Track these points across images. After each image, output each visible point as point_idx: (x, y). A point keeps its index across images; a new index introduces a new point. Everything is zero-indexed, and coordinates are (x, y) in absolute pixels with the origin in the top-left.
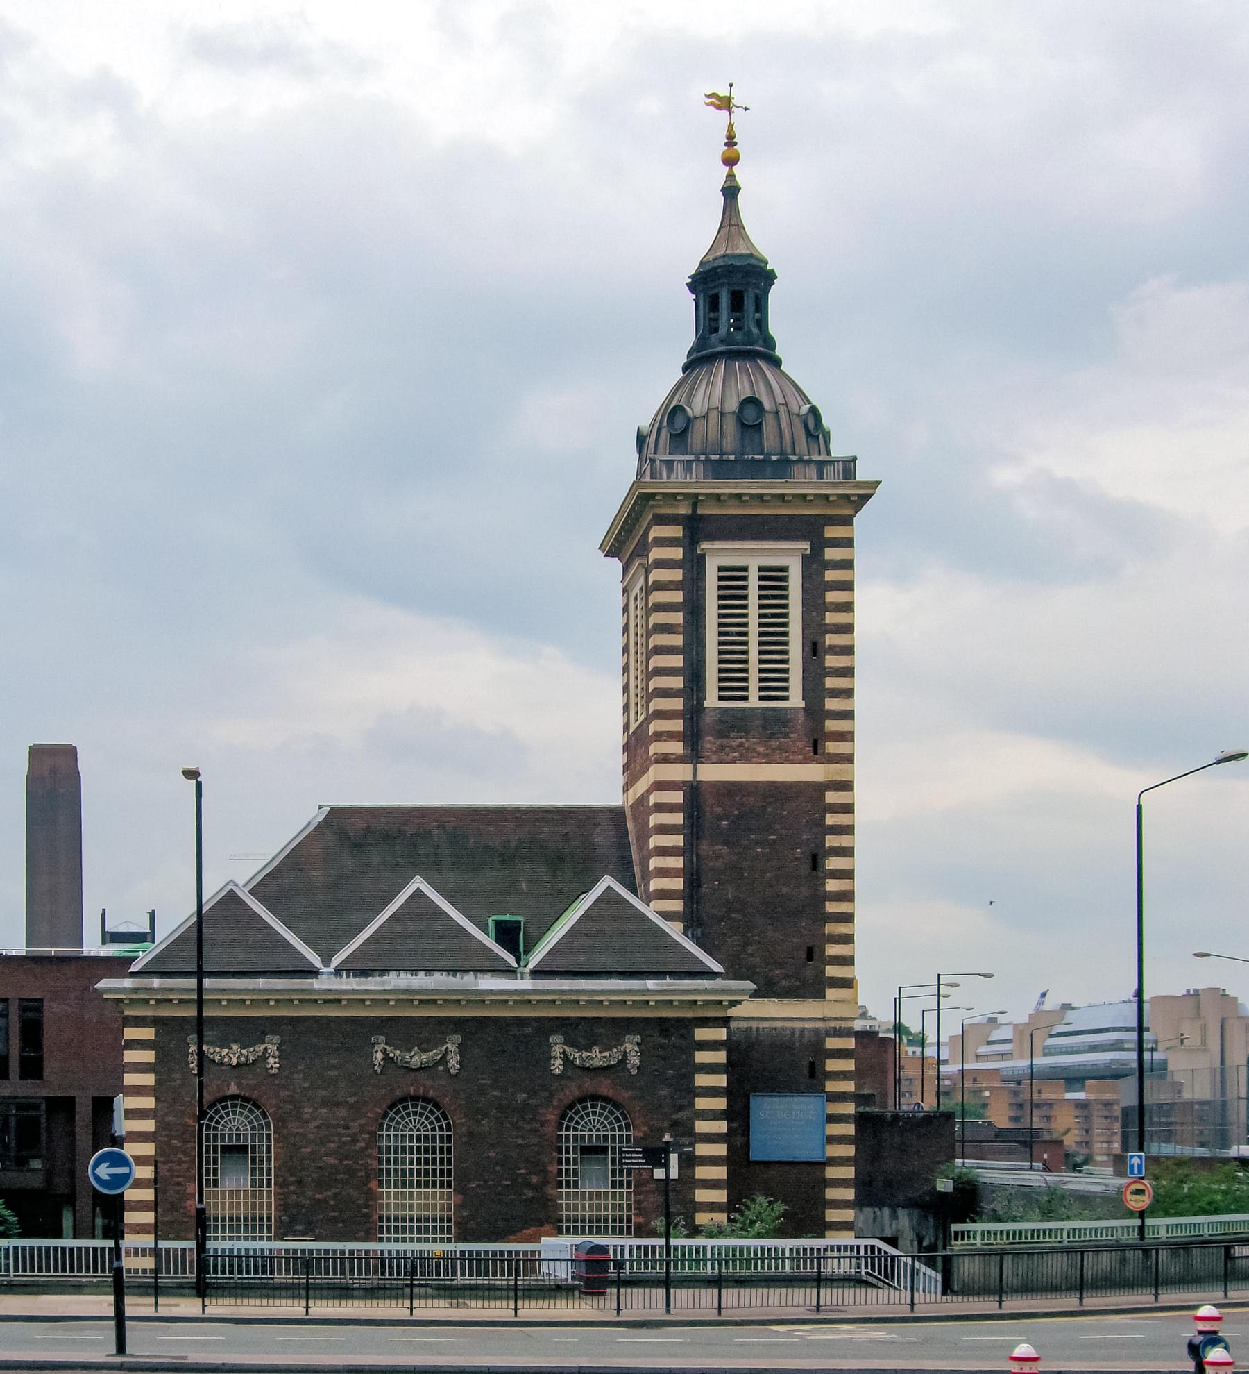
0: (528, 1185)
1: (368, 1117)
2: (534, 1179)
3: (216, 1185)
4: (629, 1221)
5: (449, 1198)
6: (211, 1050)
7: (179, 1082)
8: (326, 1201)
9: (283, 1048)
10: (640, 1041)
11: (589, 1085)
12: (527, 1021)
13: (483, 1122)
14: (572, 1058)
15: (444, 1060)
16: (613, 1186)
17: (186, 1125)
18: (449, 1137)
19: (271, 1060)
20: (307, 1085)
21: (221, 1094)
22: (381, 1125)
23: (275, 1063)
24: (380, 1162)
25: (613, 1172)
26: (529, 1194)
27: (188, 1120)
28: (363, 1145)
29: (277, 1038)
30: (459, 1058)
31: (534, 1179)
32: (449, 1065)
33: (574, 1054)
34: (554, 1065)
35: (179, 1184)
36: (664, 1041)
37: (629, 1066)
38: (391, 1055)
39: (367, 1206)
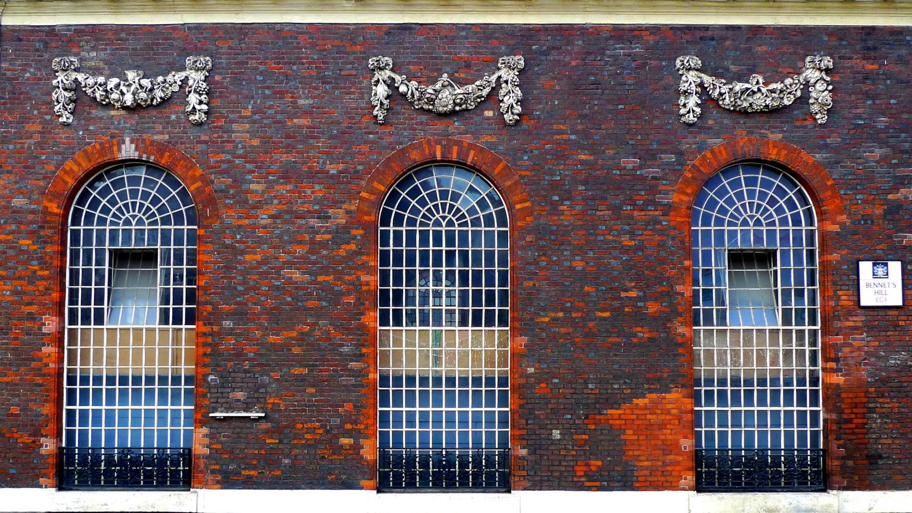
0: (639, 317)
1: (362, 199)
2: (652, 308)
3: (99, 320)
4: (814, 381)
5: (502, 344)
6: (91, 81)
7: (37, 138)
8: (287, 346)
9: (217, 78)
10: (831, 65)
11: (745, 145)
12: (636, 33)
13: (562, 208)
14: (716, 94)
15: (493, 98)
16: (786, 320)
17: (46, 212)
18: (501, 235)
19: (193, 99)
20: (256, 142)
21: (106, 159)
22: (386, 215)
23: (201, 102)
24: (384, 281)
25: (786, 294)
26: (643, 334)
27: (49, 205)
28: (353, 247)
29: (205, 60)
30: (520, 93)
31: (652, 308)
32: (504, 106)
33: (720, 88)
34: (684, 105)
35: (31, 317)
36: (871, 67)
37: (815, 108)
38: (403, 89)
39: (359, 357)
